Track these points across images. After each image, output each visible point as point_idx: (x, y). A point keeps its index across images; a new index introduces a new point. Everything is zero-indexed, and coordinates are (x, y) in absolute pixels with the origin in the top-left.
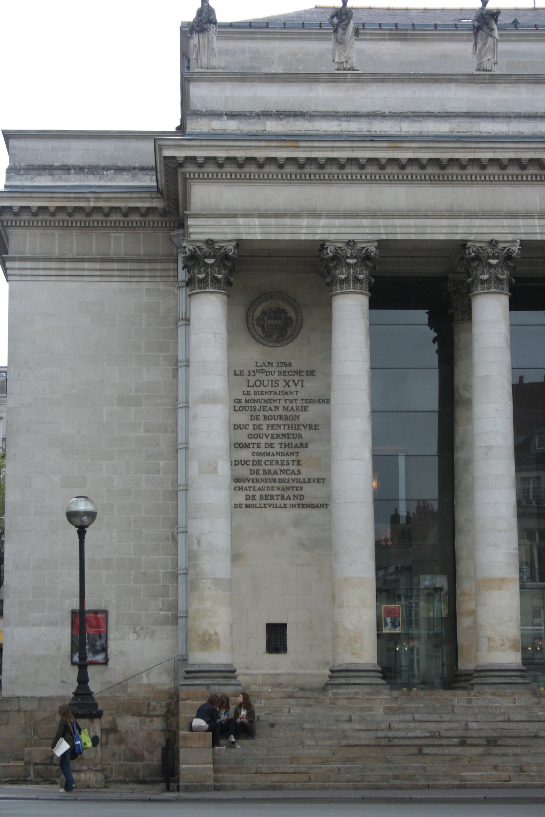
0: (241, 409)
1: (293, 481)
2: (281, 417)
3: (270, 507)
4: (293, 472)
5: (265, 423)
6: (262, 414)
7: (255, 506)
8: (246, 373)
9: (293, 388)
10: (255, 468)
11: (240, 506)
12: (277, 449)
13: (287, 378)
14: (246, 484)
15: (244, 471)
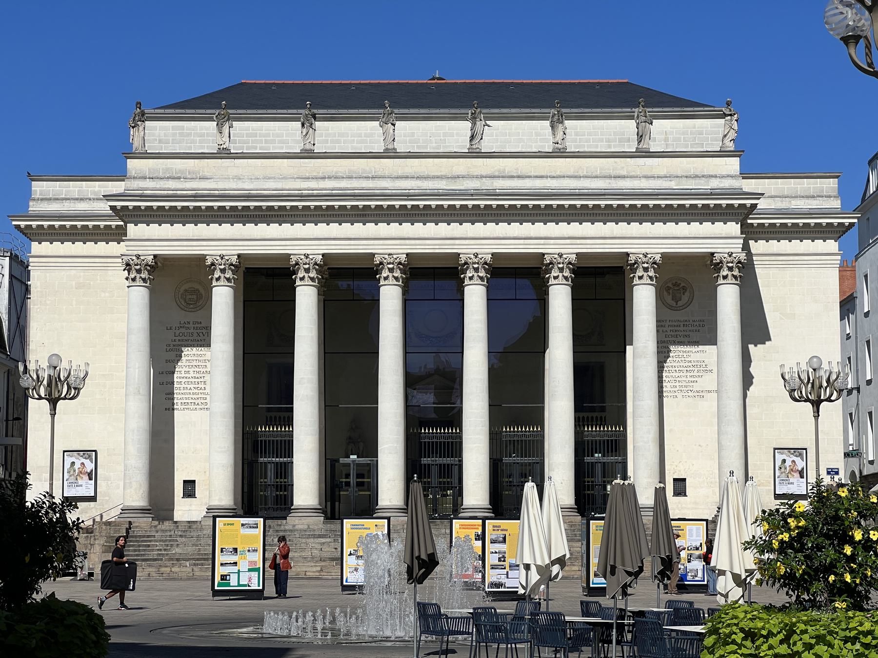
9: (202, 337)
12: (192, 375)
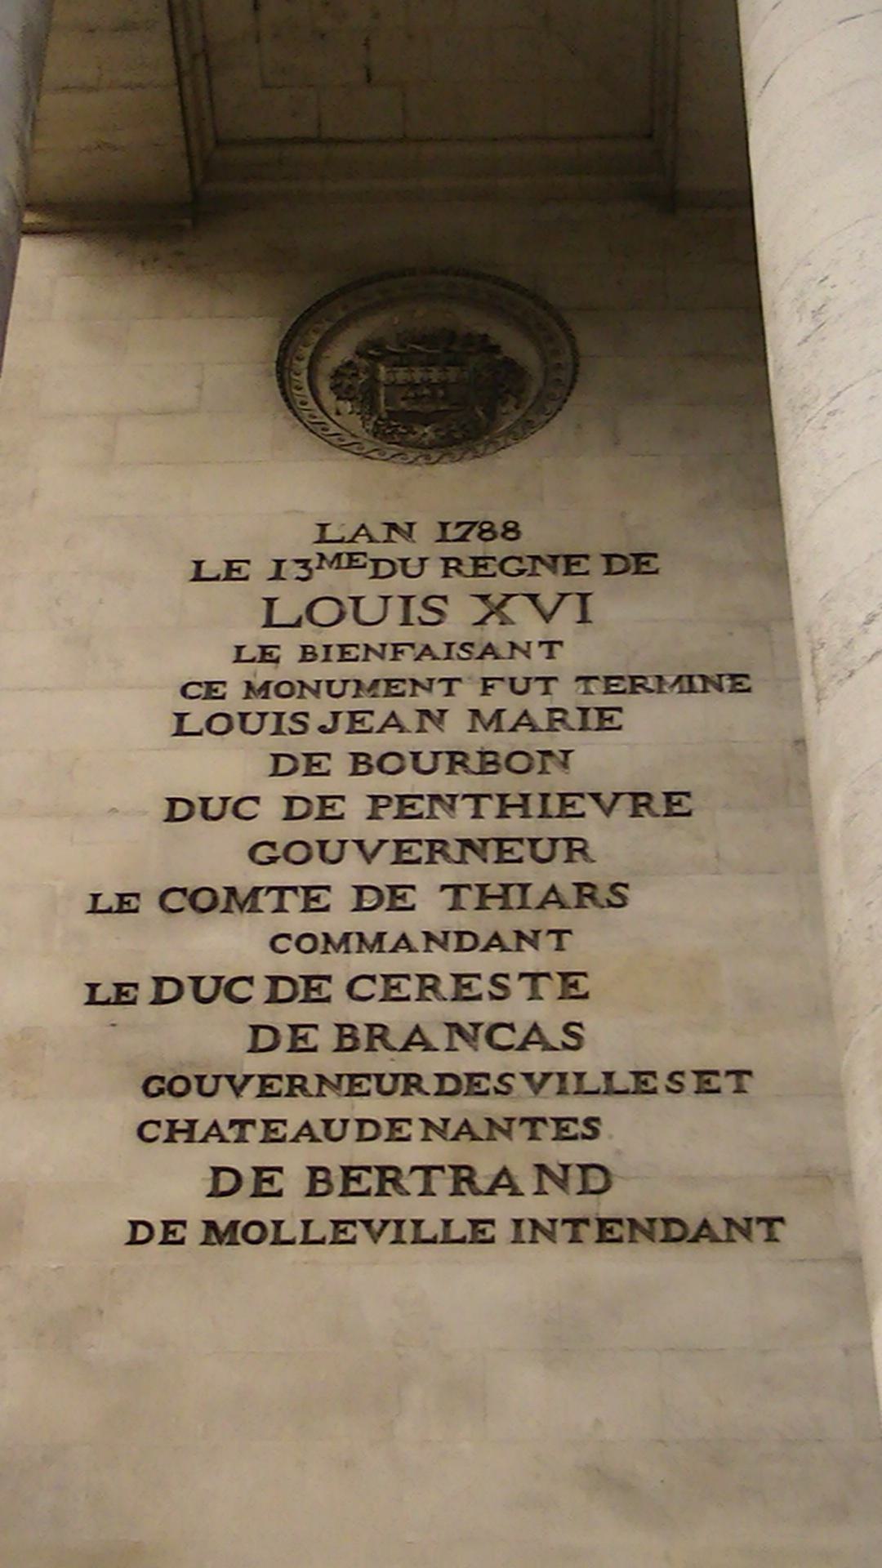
0: (219, 724)
1: (537, 1089)
2: (457, 760)
3: (375, 1237)
4: (535, 1035)
5: (356, 792)
6: (341, 744)
7: (273, 1234)
8: (261, 568)
9: (527, 626)
10: (285, 1016)
11: (171, 1232)
12: (430, 911)
13: (497, 586)
14: (224, 1107)
15: (212, 1036)
